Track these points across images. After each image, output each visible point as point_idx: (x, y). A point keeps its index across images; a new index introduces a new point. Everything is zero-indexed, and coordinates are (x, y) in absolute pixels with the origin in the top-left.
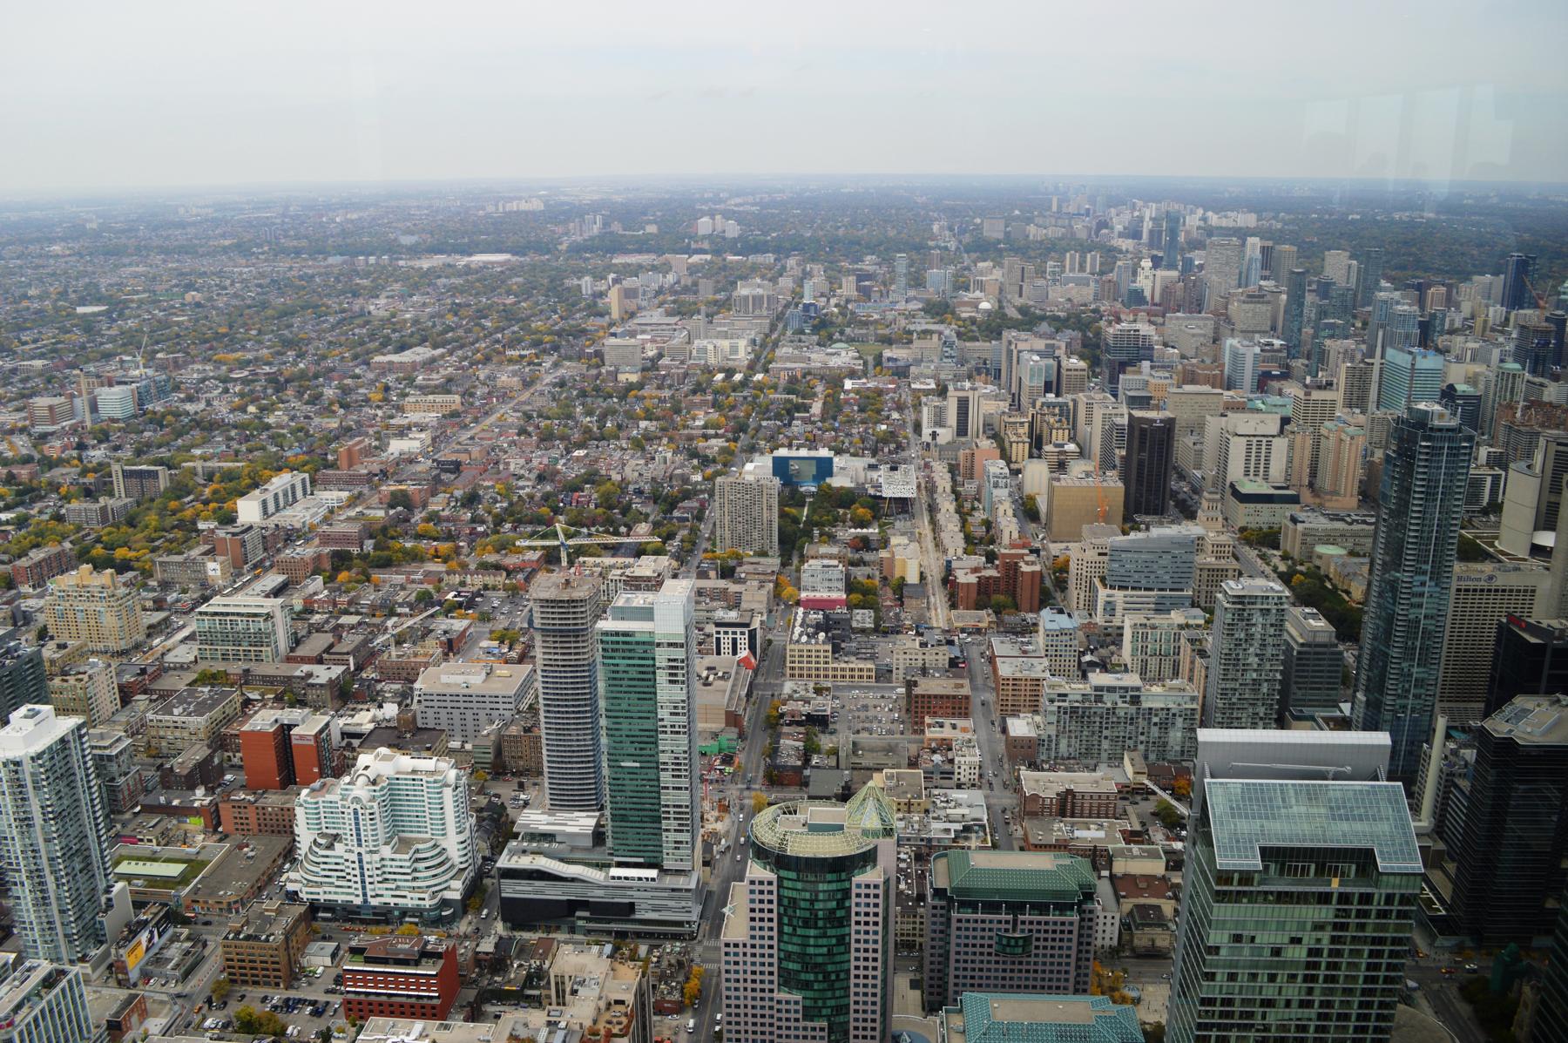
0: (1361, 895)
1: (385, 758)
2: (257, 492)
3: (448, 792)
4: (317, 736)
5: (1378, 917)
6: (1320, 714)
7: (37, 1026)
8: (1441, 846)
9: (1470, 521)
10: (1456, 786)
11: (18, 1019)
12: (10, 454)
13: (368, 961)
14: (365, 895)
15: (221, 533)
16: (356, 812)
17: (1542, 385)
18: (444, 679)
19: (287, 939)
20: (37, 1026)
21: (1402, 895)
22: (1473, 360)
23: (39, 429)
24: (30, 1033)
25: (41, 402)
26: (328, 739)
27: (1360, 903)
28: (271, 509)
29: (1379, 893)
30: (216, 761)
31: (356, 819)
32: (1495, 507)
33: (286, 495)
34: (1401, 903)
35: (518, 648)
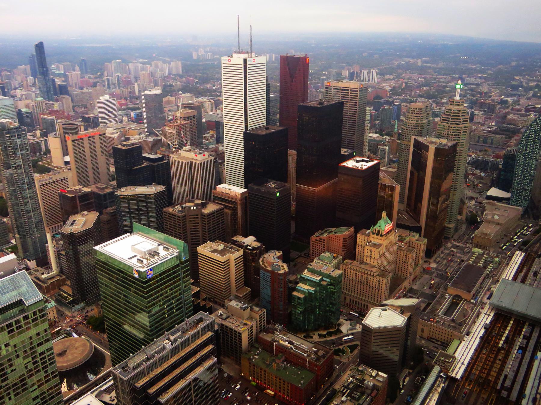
0: (23, 317)
5: (33, 322)
6: (4, 248)
8: (64, 277)
9: (41, 158)
10: (61, 254)
17: (52, 104)
21: (39, 310)
22: (26, 99)
27: (24, 320)
29: (30, 313)
32: (48, 151)
34: (40, 313)
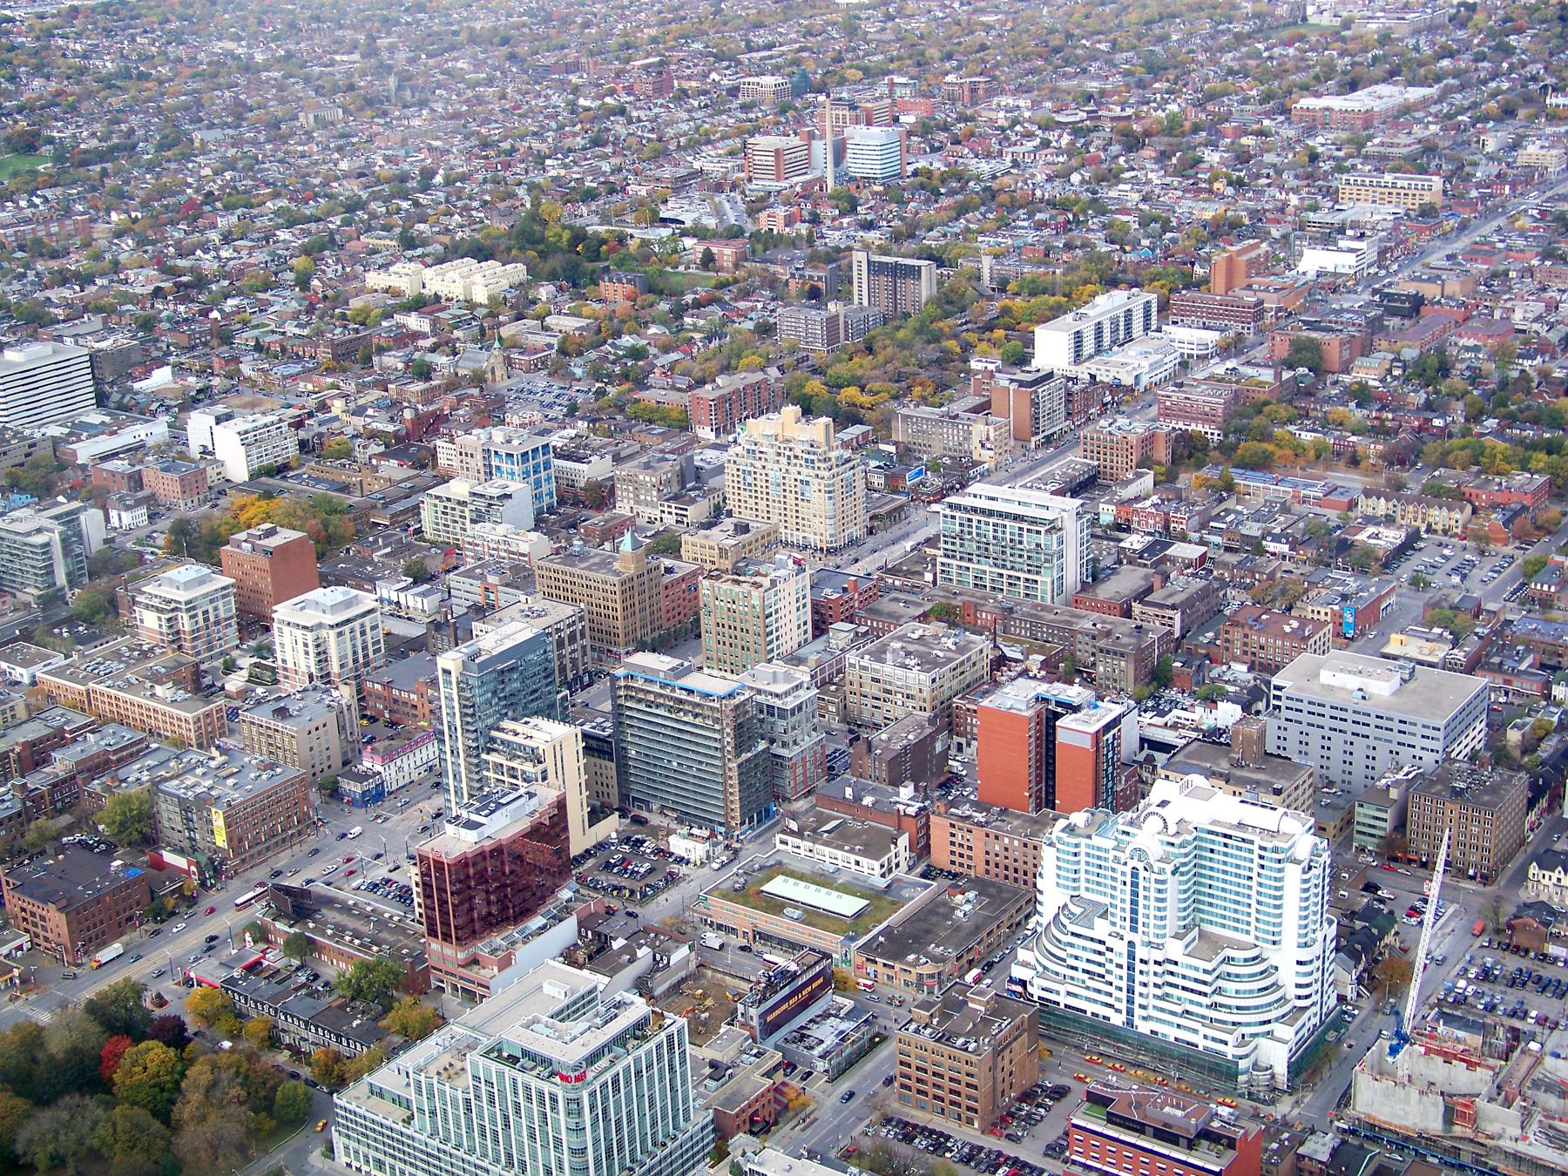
1: (1193, 793)
2: (1069, 317)
3: (1293, 874)
4: (1097, 736)
7: (616, 1090)
11: (590, 1075)
12: (711, 222)
13: (1112, 1119)
14: (1130, 1012)
15: (1003, 380)
16: (1135, 875)
18: (1326, 677)
19: (998, 1052)
20: (616, 1090)
23: (758, 186)
24: (605, 1098)
25: (765, 143)
26: (1114, 746)
28: (1089, 346)
30: (939, 747)
31: (1135, 885)
33: (1114, 322)
35: (1471, 645)
